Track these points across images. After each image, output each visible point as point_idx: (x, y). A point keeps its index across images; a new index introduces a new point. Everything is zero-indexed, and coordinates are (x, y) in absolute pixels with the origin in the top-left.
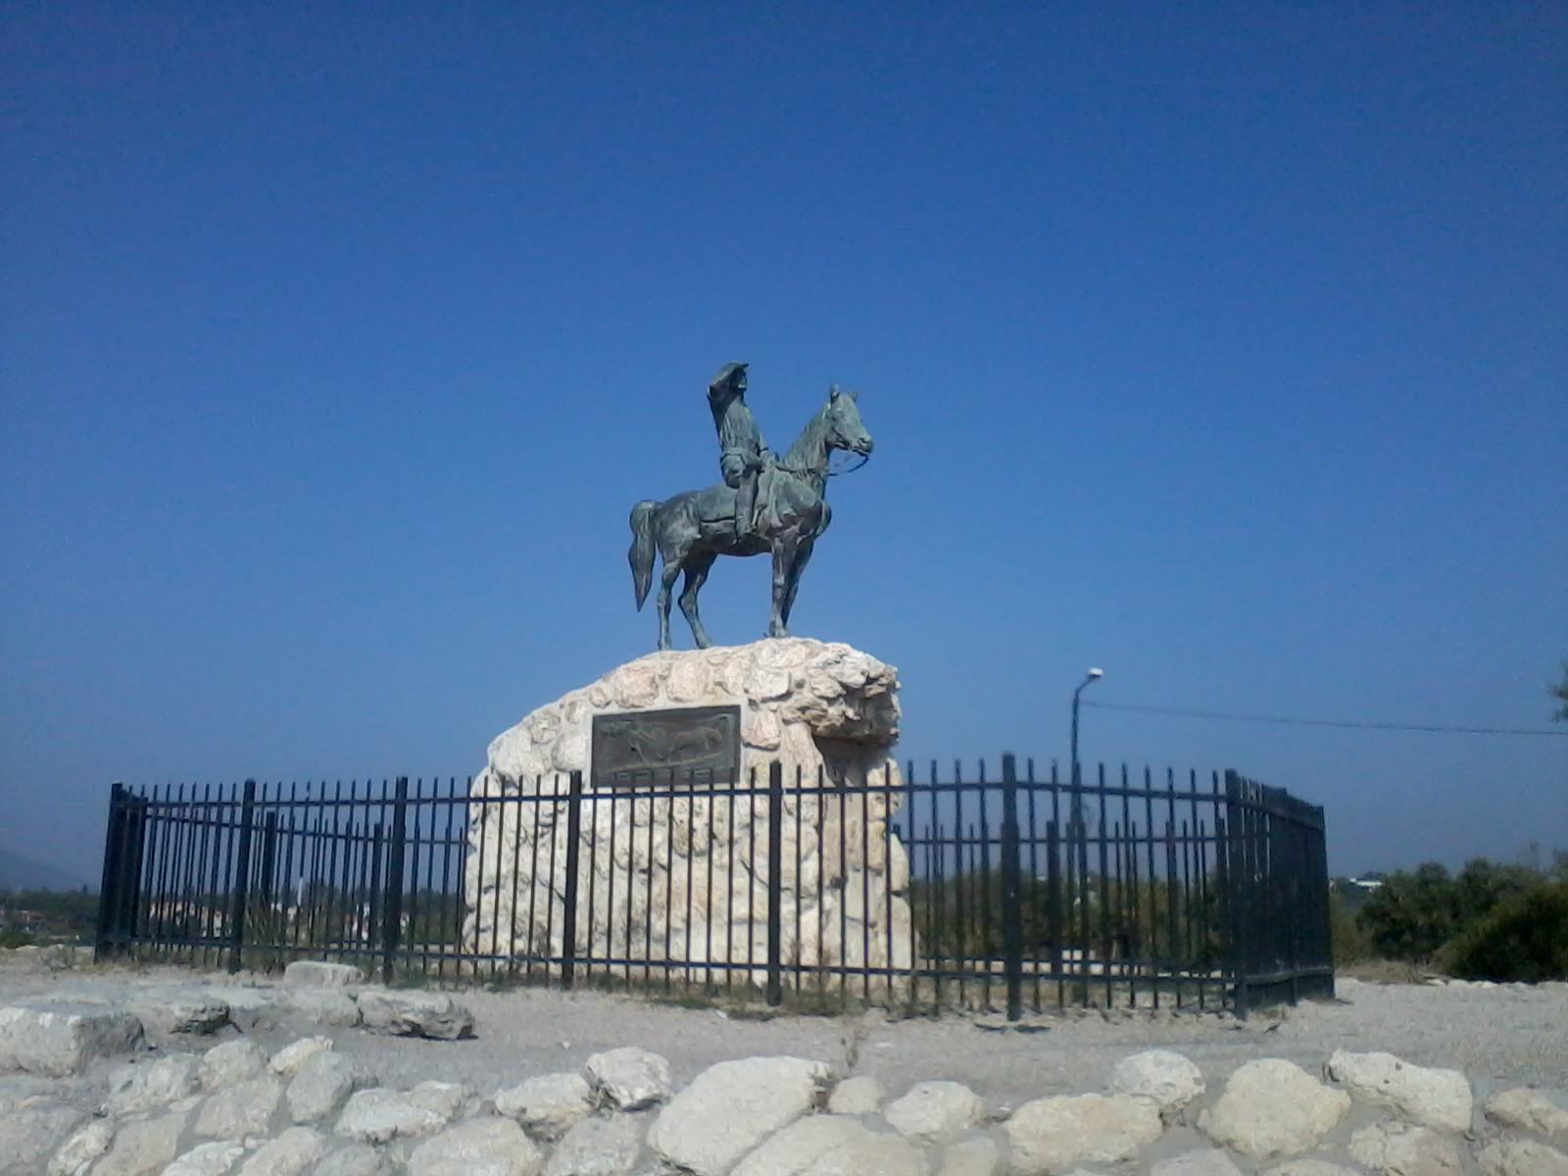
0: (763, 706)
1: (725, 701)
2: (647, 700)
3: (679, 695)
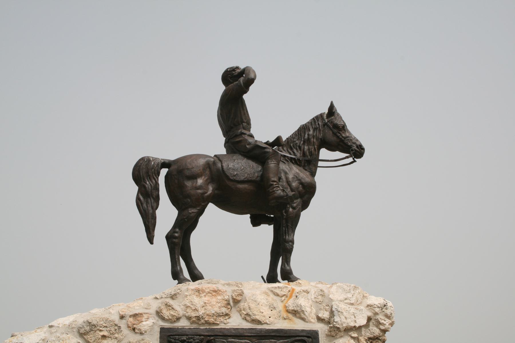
1: (298, 325)
2: (222, 319)
3: (258, 317)
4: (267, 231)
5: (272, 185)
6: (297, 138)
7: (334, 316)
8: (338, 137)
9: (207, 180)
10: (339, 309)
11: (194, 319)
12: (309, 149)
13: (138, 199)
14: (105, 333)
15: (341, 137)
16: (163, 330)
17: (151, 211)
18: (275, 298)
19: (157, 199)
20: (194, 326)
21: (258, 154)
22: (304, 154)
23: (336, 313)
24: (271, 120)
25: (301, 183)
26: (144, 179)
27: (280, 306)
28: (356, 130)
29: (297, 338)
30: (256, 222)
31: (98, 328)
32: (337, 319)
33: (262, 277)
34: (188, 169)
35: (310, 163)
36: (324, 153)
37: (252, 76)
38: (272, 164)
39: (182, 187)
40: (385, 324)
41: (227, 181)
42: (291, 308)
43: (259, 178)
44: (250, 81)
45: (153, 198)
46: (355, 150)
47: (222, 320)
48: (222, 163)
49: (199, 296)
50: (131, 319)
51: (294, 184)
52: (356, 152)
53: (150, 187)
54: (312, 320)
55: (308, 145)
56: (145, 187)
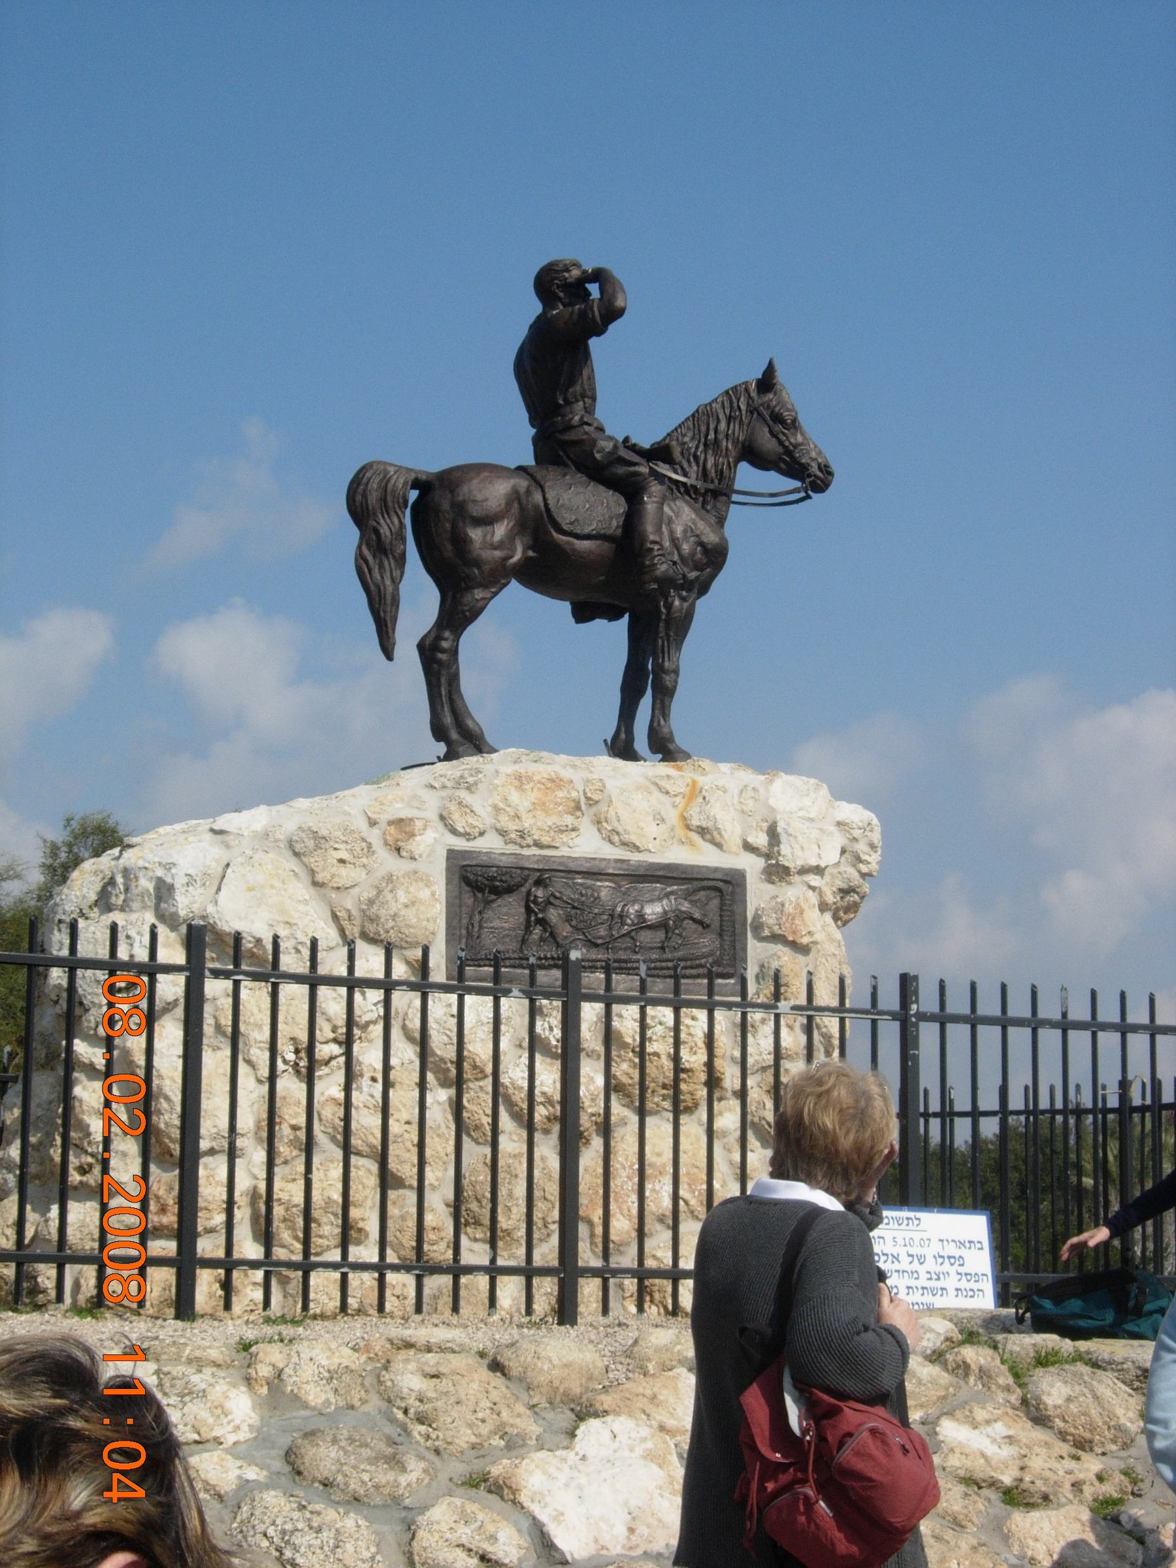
0: (797, 878)
1: (704, 857)
4: (611, 638)
5: (651, 550)
6: (690, 434)
7: (778, 843)
8: (781, 443)
9: (512, 529)
10: (790, 831)
11: (513, 836)
12: (716, 465)
13: (360, 556)
14: (344, 855)
15: (787, 443)
16: (452, 854)
17: (390, 589)
18: (663, 797)
19: (401, 560)
20: (512, 849)
21: (621, 473)
22: (705, 474)
23: (783, 838)
25: (701, 544)
26: (374, 514)
27: (673, 816)
28: (820, 434)
29: (706, 883)
30: (583, 613)
31: (332, 843)
32: (785, 849)
33: (605, 741)
34: (475, 501)
35: (714, 495)
36: (747, 476)
38: (650, 503)
39: (460, 542)
40: (869, 863)
41: (554, 534)
42: (695, 822)
43: (620, 530)
45: (394, 557)
46: (815, 476)
47: (565, 840)
48: (543, 491)
49: (520, 788)
50: (392, 829)
51: (686, 548)
52: (814, 479)
53: (388, 534)
54: (734, 849)
55: (715, 454)
56: (377, 532)
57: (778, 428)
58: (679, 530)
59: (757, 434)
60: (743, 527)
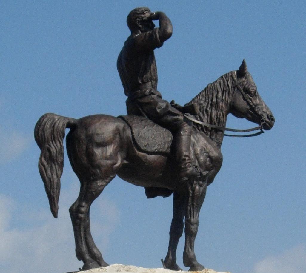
6: (204, 99)
8: (248, 104)
9: (116, 149)
12: (217, 115)
13: (41, 164)
15: (251, 104)
19: (61, 165)
21: (169, 119)
22: (211, 120)
24: (177, 79)
25: (209, 157)
26: (48, 141)
28: (268, 99)
34: (98, 134)
35: (216, 131)
37: (169, 30)
38: (184, 135)
39: (90, 156)
41: (137, 151)
43: (169, 150)
44: (165, 36)
45: (58, 164)
46: (266, 121)
48: (131, 129)
51: (202, 158)
52: (265, 123)
53: (55, 151)
55: (216, 109)
57: (248, 96)
58: (198, 149)
59: (236, 99)
60: (230, 148)
